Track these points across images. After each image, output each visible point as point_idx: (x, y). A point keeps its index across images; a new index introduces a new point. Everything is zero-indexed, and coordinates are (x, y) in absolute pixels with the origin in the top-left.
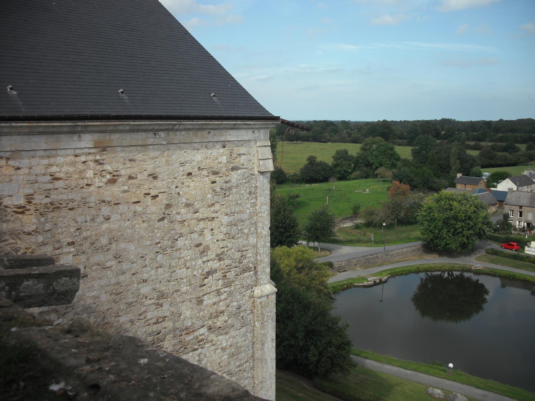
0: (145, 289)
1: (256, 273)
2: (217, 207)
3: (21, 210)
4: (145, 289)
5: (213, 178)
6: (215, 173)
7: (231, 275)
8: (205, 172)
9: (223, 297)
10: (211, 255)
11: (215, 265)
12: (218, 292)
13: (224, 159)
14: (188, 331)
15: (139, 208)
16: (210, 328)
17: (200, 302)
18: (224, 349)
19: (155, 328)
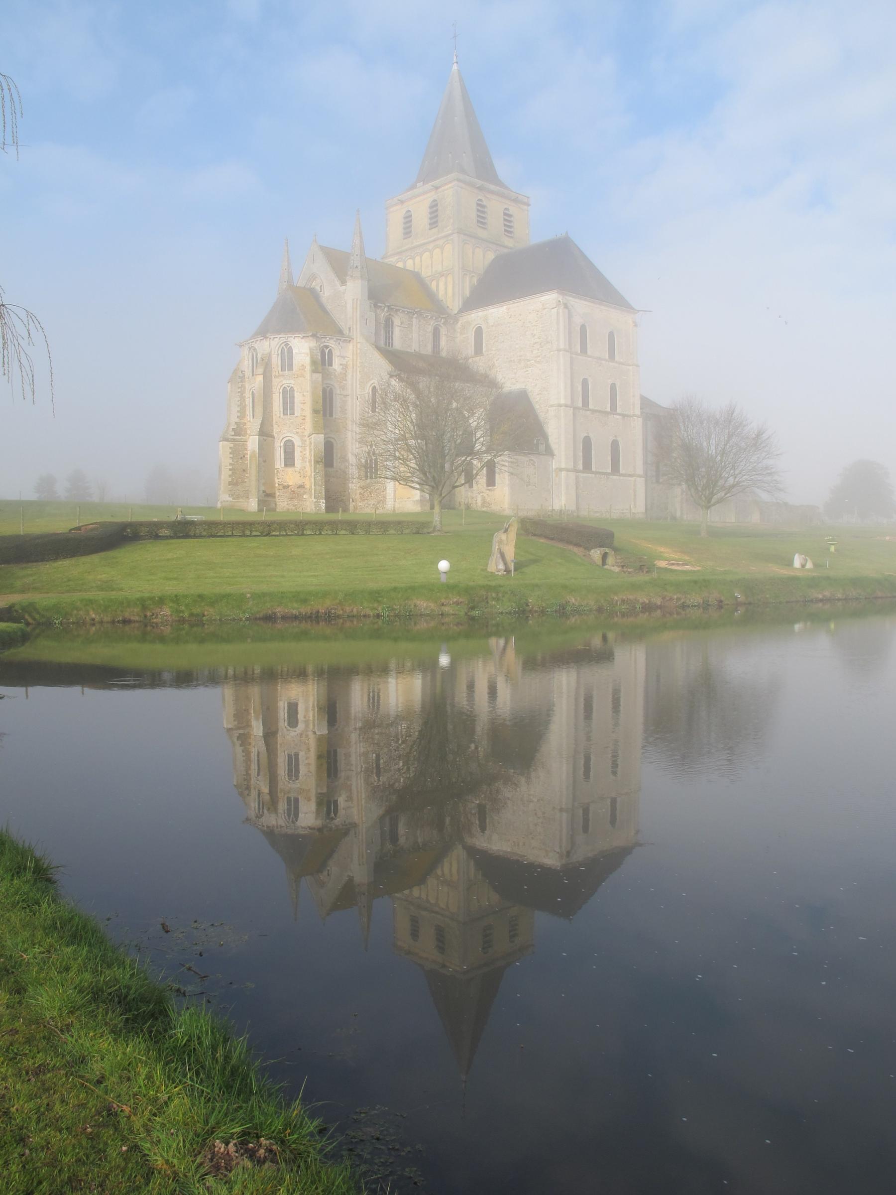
0: (517, 346)
1: (552, 343)
2: (538, 322)
3: (492, 326)
4: (517, 346)
5: (537, 313)
6: (538, 311)
7: (542, 344)
8: (534, 312)
9: (540, 351)
10: (536, 337)
11: (538, 340)
12: (538, 350)
13: (541, 307)
14: (529, 361)
15: (516, 324)
16: (535, 361)
17: (532, 352)
18: (540, 369)
19: (519, 358)
